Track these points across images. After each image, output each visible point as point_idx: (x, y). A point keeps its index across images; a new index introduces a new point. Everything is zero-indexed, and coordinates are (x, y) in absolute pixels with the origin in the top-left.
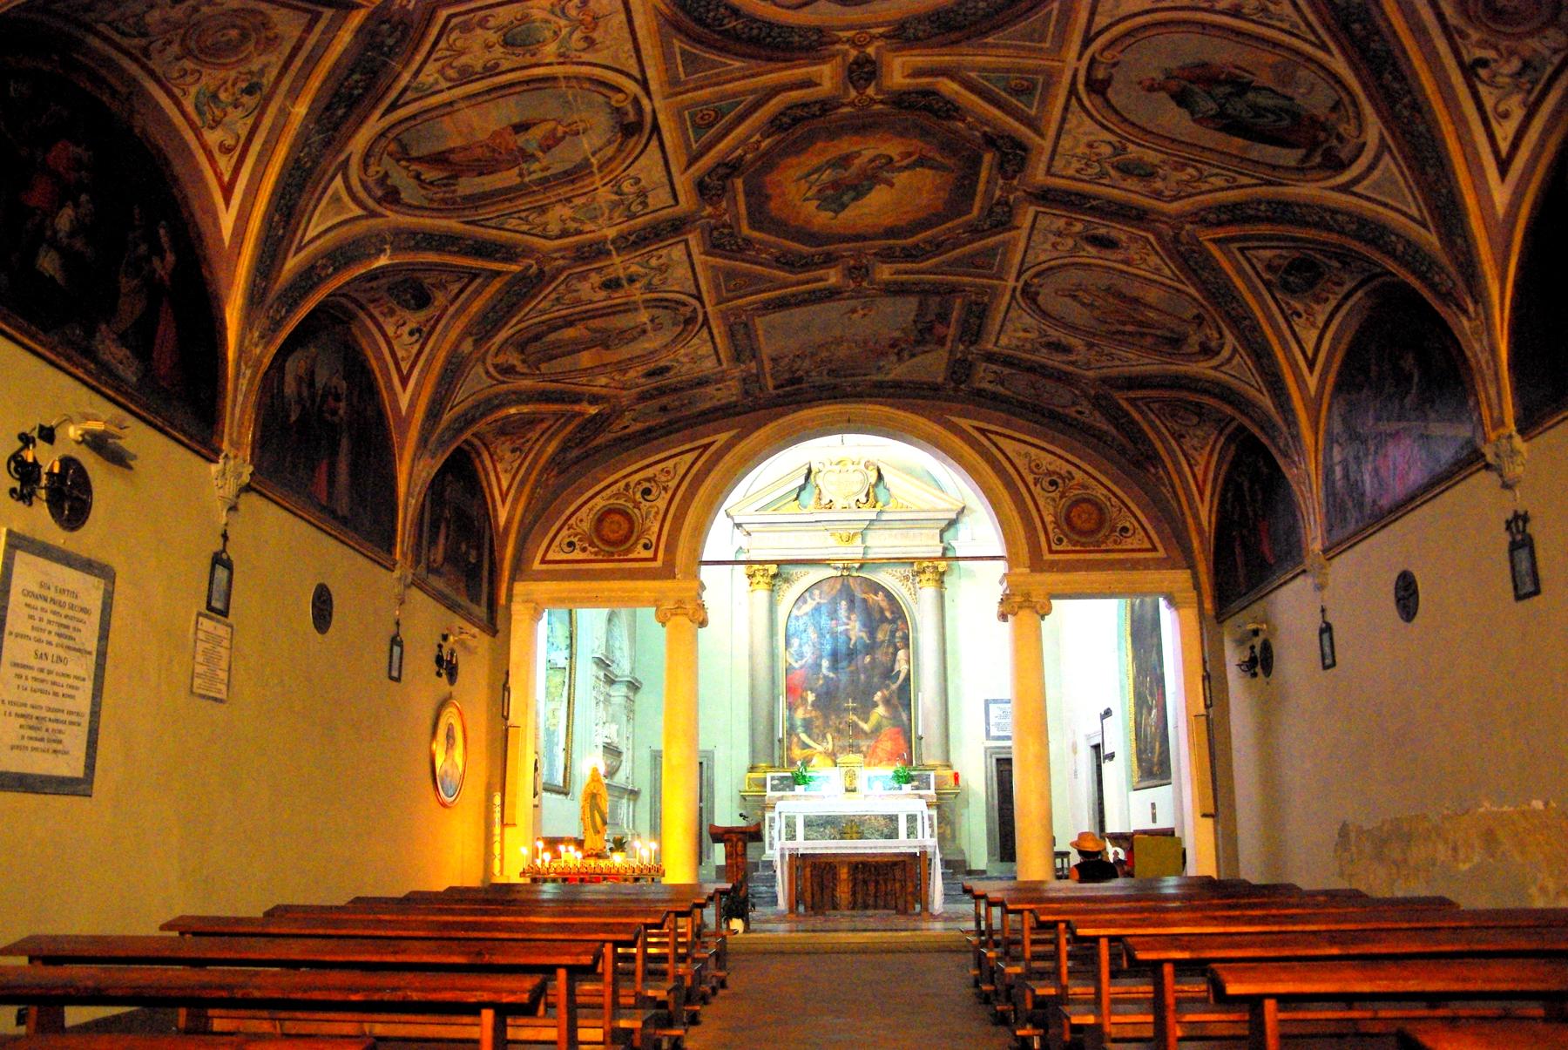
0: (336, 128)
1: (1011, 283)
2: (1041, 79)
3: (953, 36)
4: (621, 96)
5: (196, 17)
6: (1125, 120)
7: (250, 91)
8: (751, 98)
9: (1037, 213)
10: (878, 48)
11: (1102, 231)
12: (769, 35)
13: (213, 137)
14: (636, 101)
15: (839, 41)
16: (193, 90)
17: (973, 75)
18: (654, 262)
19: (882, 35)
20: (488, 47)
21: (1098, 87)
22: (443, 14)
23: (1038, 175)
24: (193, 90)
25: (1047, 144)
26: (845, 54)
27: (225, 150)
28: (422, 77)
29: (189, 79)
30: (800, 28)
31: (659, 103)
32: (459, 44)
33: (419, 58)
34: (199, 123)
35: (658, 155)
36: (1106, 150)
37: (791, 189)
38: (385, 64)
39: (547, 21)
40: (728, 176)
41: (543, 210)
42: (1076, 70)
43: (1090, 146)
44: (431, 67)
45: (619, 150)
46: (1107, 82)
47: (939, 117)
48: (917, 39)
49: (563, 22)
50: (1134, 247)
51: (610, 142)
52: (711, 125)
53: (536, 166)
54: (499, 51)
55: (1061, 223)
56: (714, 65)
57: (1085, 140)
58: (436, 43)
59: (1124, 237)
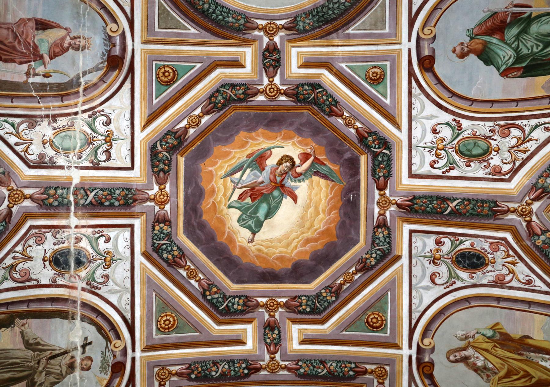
1: (405, 351)
2: (388, 64)
3: (328, 27)
4: (114, 27)
6: (454, 94)
8: (198, 65)
9: (411, 232)
10: (281, 37)
11: (467, 245)
12: (214, 12)
14: (123, 35)
15: (257, 28)
17: (343, 65)
18: (102, 246)
19: (283, 27)
21: (427, 63)
23: (405, 183)
25: (403, 136)
26: (261, 38)
30: (235, 12)
31: (139, 46)
35: (128, 95)
36: (447, 133)
37: (219, 184)
40: (172, 149)
41: (32, 121)
42: (410, 51)
43: (434, 131)
45: (102, 79)
46: (431, 59)
47: (323, 111)
48: (305, 31)
50: (499, 256)
51: (97, 69)
52: (169, 83)
53: (40, 69)
55: (431, 242)
56: (178, 26)
57: (429, 124)
59: (487, 246)
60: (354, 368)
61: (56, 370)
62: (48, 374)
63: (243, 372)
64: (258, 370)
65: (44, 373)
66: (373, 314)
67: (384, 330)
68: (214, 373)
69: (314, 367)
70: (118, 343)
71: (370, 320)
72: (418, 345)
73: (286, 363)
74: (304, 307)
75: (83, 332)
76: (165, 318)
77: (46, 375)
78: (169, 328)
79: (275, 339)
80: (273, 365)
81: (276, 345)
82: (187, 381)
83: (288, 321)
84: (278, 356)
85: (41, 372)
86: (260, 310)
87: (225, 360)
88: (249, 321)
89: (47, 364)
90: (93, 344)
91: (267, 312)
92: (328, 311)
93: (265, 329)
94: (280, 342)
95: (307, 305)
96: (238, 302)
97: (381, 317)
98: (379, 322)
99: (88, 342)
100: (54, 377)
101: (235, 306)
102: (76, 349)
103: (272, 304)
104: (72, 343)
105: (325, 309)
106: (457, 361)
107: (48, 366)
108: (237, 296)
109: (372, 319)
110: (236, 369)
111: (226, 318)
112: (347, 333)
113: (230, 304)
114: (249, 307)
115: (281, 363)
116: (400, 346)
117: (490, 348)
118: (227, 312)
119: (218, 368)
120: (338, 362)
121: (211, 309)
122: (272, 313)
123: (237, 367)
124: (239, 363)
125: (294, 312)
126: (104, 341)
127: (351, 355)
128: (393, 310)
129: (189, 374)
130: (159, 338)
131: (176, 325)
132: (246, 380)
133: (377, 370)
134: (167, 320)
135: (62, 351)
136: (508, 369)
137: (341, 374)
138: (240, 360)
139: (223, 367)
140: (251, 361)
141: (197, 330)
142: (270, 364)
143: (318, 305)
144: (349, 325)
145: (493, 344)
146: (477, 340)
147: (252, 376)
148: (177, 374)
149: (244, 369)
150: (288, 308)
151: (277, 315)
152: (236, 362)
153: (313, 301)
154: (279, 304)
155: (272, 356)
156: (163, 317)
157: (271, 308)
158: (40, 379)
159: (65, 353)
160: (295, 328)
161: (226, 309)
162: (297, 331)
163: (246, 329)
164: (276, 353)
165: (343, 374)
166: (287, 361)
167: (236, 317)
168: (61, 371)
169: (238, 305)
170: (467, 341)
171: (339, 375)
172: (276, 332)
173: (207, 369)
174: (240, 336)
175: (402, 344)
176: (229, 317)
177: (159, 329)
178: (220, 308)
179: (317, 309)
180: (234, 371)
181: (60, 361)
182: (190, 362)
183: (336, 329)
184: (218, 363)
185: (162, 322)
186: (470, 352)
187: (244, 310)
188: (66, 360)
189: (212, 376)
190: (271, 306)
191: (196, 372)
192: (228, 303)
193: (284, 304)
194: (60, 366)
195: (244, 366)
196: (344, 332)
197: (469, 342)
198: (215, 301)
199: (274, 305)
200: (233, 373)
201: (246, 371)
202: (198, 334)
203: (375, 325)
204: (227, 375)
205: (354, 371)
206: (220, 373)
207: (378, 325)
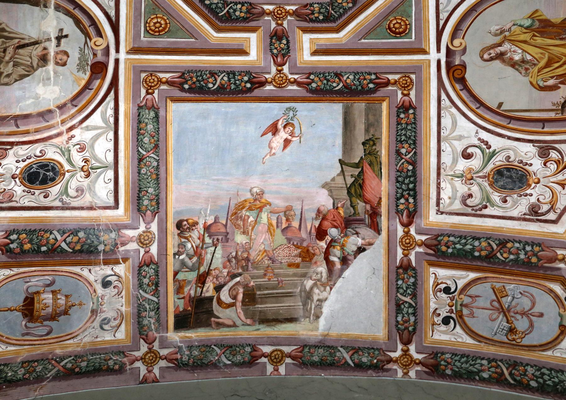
60: (374, 79)
61: (26, 60)
62: (16, 65)
63: (245, 86)
64: (262, 84)
65: (12, 63)
66: (396, 19)
67: (408, 35)
68: (210, 85)
69: (328, 81)
70: (100, 41)
71: (392, 25)
72: (447, 47)
73: (296, 77)
74: (316, 15)
75: (58, 23)
76: (155, 21)
77: (14, 66)
78: (159, 32)
79: (283, 50)
80: (281, 79)
81: (284, 56)
82: (178, 91)
83: (297, 30)
84: (286, 69)
85: (8, 62)
86: (266, 18)
87: (225, 72)
88: (253, 30)
89: (15, 53)
90: (70, 37)
91: (274, 21)
92: (344, 18)
93: (271, 39)
94: (289, 52)
95: (320, 13)
96: (240, 9)
97: (404, 21)
98: (403, 27)
99: (64, 34)
100: (23, 69)
101: (237, 13)
102: (49, 40)
103: (279, 12)
104: (44, 33)
105: (341, 16)
106: (492, 59)
107: (16, 56)
108: (240, 3)
109: (394, 24)
110: (237, 82)
111: (227, 25)
112: (366, 41)
113: (231, 11)
114: (254, 14)
115: (290, 76)
116: (427, 50)
117: (528, 39)
118: (228, 18)
119: (216, 80)
120: (356, 74)
121: (209, 15)
122: (279, 22)
123: (238, 80)
124: (240, 75)
125: (306, 20)
126: (82, 37)
127: (370, 65)
128: (418, 13)
129: (182, 84)
130: (147, 41)
131: (167, 29)
132: (248, 95)
133: (401, 80)
134: (157, 22)
135: (33, 40)
136: (549, 57)
137: (360, 88)
138: (241, 72)
139: (222, 78)
140: (255, 73)
141: (193, 36)
142: (277, 78)
143: (333, 12)
144: (368, 32)
145: (531, 34)
146: (514, 32)
147: (256, 91)
148: (167, 82)
149: (246, 82)
150: (298, 16)
151: (285, 24)
152: (237, 74)
153: (327, 9)
154: (288, 13)
155: (280, 68)
156: (153, 19)
157: (278, 16)
158: (6, 69)
159: (36, 43)
160: (306, 38)
161: (227, 15)
162: (309, 41)
163: (249, 38)
164: (284, 64)
165: (362, 87)
166: (296, 74)
167: (238, 24)
168: (31, 63)
169: (241, 12)
170: (502, 36)
171: (357, 88)
172: (284, 41)
173: (203, 80)
174: (242, 45)
175: (429, 49)
176: (230, 25)
177: (148, 31)
178: (220, 15)
179: (331, 16)
180: (235, 84)
181: (30, 51)
182: (183, 70)
183: (353, 37)
184: (216, 74)
185: (152, 24)
186: (506, 46)
187: (247, 18)
188: (37, 51)
189: (209, 88)
190: (278, 14)
191: (190, 82)
192: (229, 9)
193: (294, 12)
194: (31, 58)
195: (246, 78)
196: (363, 41)
197: (505, 36)
198: (214, 6)
199: (282, 13)
200: (233, 87)
201: (248, 85)
202: (193, 40)
203: (397, 30)
204: (226, 89)
205: (374, 83)
206: (219, 86)
207: (401, 30)
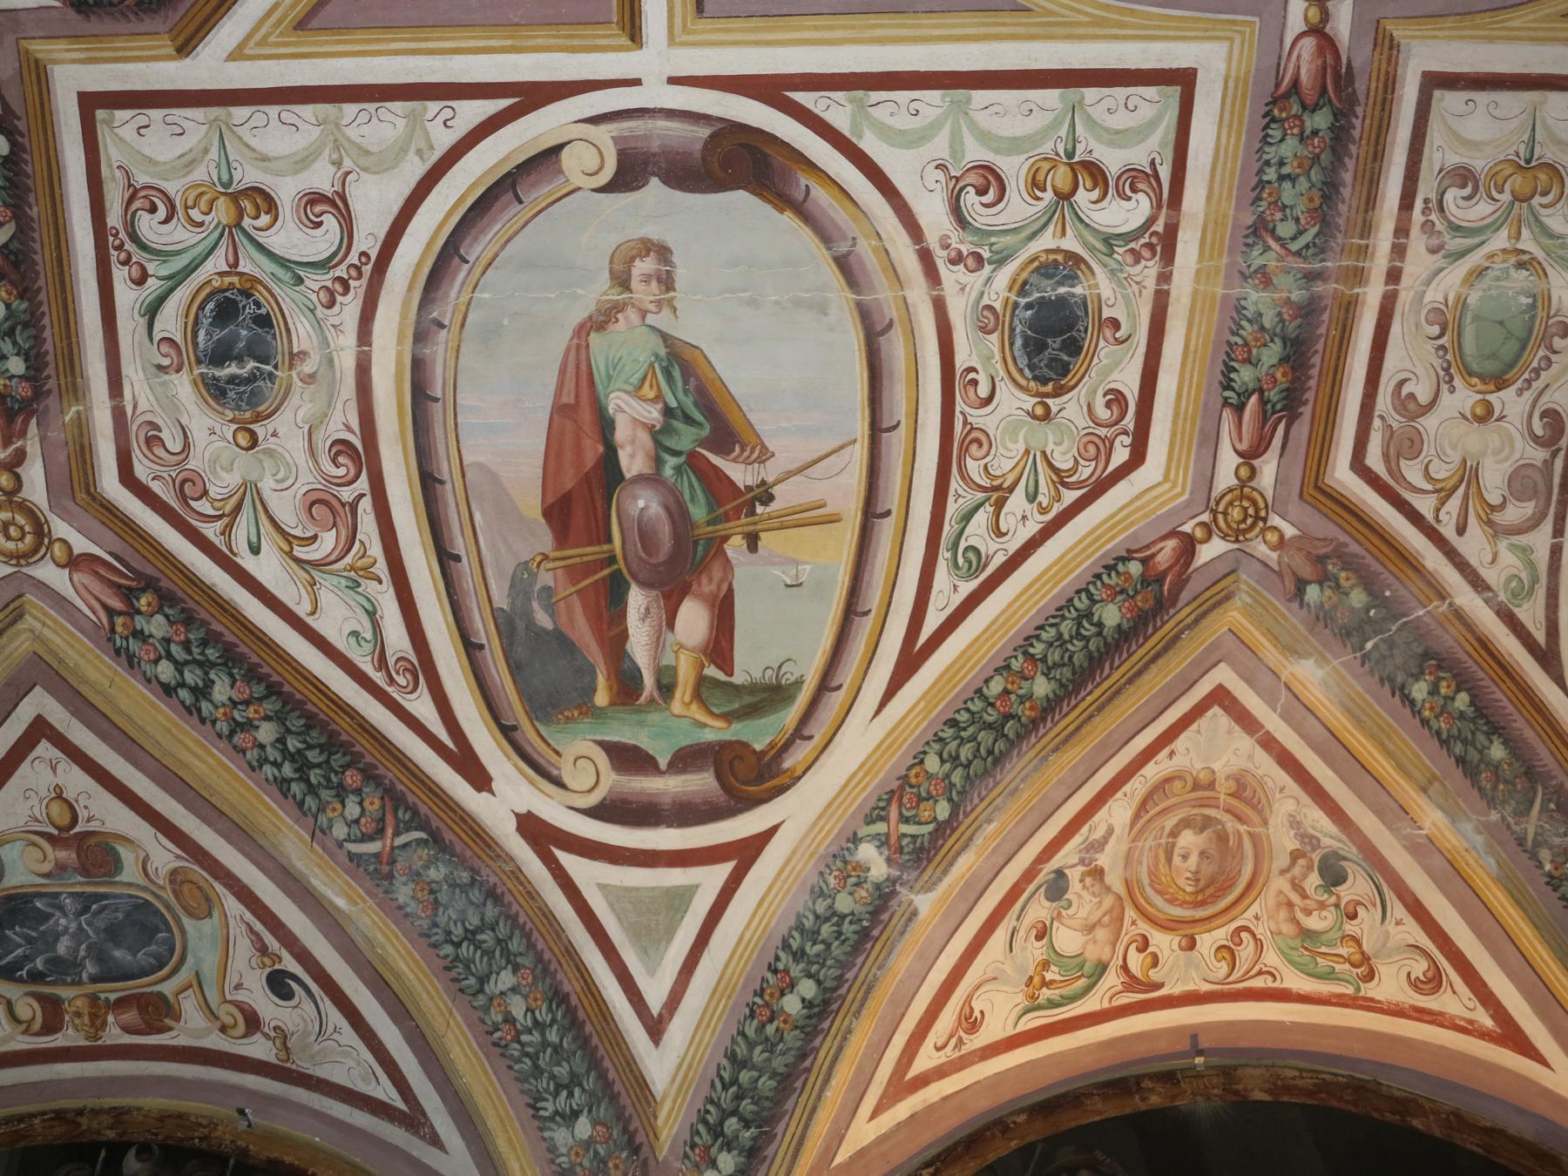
0: (1531, 774)
5: (1114, 879)
7: (1333, 876)
13: (1390, 985)
16: (1271, 958)
20: (1485, 415)
22: (1342, 474)
24: (1271, 958)
27: (1433, 982)
28: (1490, 575)
29: (1246, 952)
32: (1440, 471)
33: (1432, 558)
34: (1350, 990)
38: (1416, 628)
39: (1479, 273)
44: (1473, 545)
49: (1500, 241)
54: (1511, 402)
58: (1415, 517)
